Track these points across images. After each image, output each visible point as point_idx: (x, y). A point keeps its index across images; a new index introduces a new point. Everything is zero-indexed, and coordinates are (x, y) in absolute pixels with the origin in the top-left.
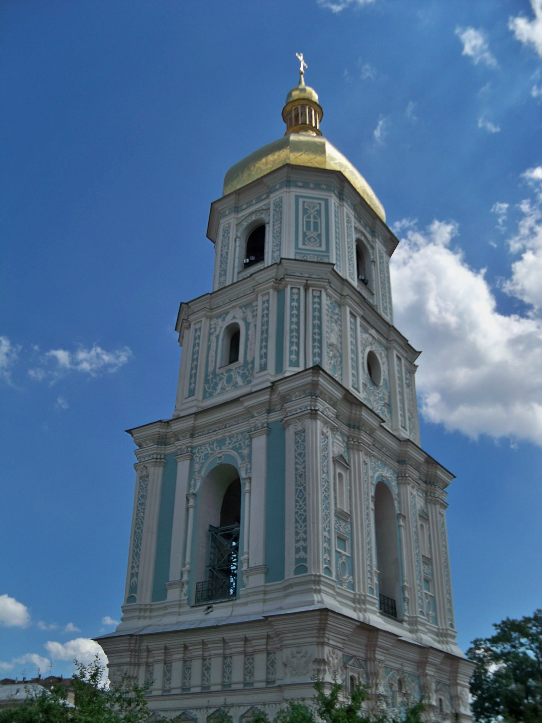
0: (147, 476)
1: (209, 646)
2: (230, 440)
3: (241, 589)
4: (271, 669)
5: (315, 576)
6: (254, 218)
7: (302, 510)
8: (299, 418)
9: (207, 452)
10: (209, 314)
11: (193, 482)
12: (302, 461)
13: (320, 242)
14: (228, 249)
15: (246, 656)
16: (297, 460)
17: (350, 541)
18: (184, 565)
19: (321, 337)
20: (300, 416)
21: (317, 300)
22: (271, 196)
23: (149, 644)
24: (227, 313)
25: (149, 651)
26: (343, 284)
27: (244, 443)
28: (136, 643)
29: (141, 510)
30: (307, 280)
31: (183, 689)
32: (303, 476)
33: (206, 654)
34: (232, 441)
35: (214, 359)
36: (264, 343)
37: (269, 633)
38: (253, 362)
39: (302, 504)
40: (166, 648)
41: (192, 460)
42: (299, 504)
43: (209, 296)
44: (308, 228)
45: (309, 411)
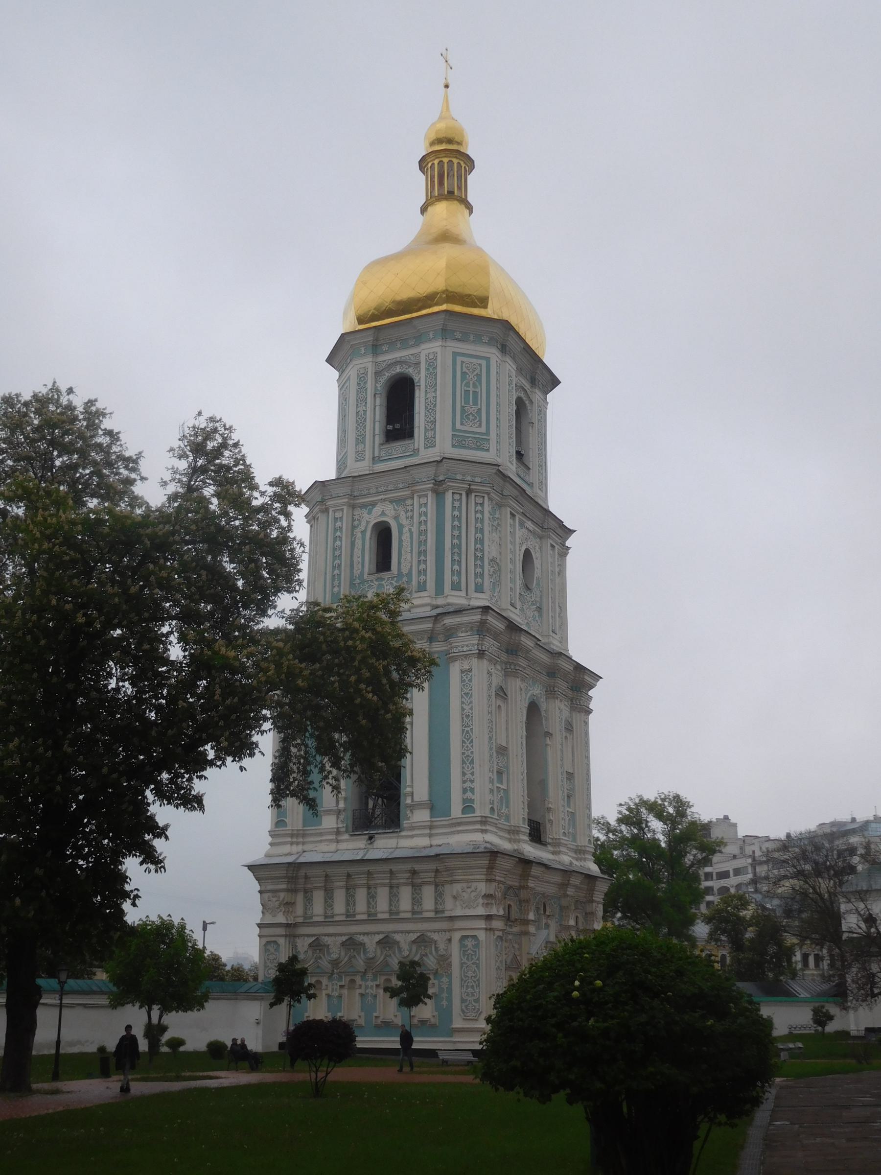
1: (375, 876)
3: (405, 822)
4: (439, 899)
5: (482, 816)
6: (398, 369)
7: (469, 752)
8: (466, 656)
13: (480, 421)
14: (365, 406)
15: (413, 886)
17: (506, 772)
19: (483, 554)
21: (479, 508)
22: (423, 346)
23: (307, 872)
24: (374, 504)
25: (306, 877)
26: (504, 481)
28: (294, 871)
30: (470, 485)
31: (347, 916)
32: (470, 718)
33: (372, 882)
35: (360, 559)
36: (422, 558)
37: (438, 868)
38: (410, 574)
39: (469, 745)
40: (327, 876)
42: (466, 745)
43: (351, 479)
44: (467, 402)
45: (477, 651)
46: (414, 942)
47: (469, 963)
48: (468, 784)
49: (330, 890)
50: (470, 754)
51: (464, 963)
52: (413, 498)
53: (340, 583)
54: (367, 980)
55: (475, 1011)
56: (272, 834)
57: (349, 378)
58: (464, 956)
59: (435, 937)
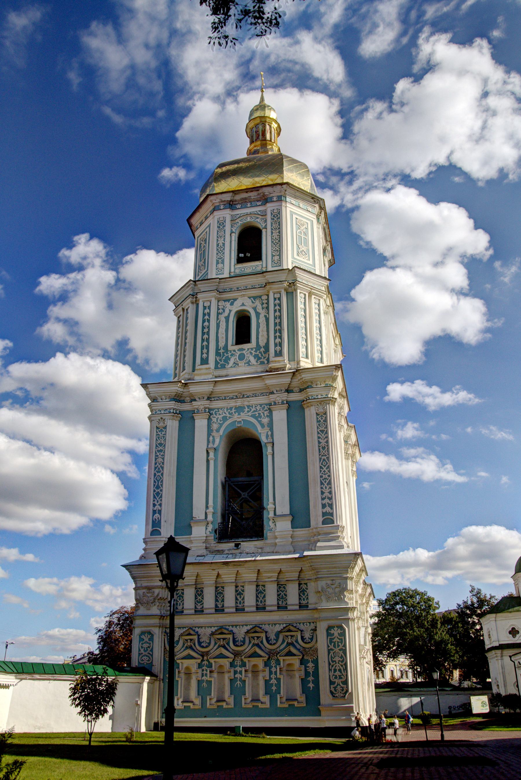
0: (165, 428)
2: (248, 408)
6: (249, 219)
7: (327, 475)
9: (224, 415)
10: (218, 296)
11: (211, 438)
12: (324, 437)
14: (224, 240)
16: (319, 435)
18: (207, 507)
20: (322, 401)
22: (268, 205)
27: (263, 413)
29: (160, 456)
32: (326, 449)
34: (251, 409)
35: (224, 336)
38: (267, 347)
39: (326, 470)
41: (209, 419)
43: (218, 280)
46: (281, 632)
47: (337, 650)
48: (326, 501)
49: (200, 588)
50: (327, 477)
51: (332, 649)
52: (268, 295)
53: (208, 351)
54: (236, 666)
55: (344, 692)
56: (145, 541)
57: (209, 226)
58: (331, 642)
59: (302, 627)
